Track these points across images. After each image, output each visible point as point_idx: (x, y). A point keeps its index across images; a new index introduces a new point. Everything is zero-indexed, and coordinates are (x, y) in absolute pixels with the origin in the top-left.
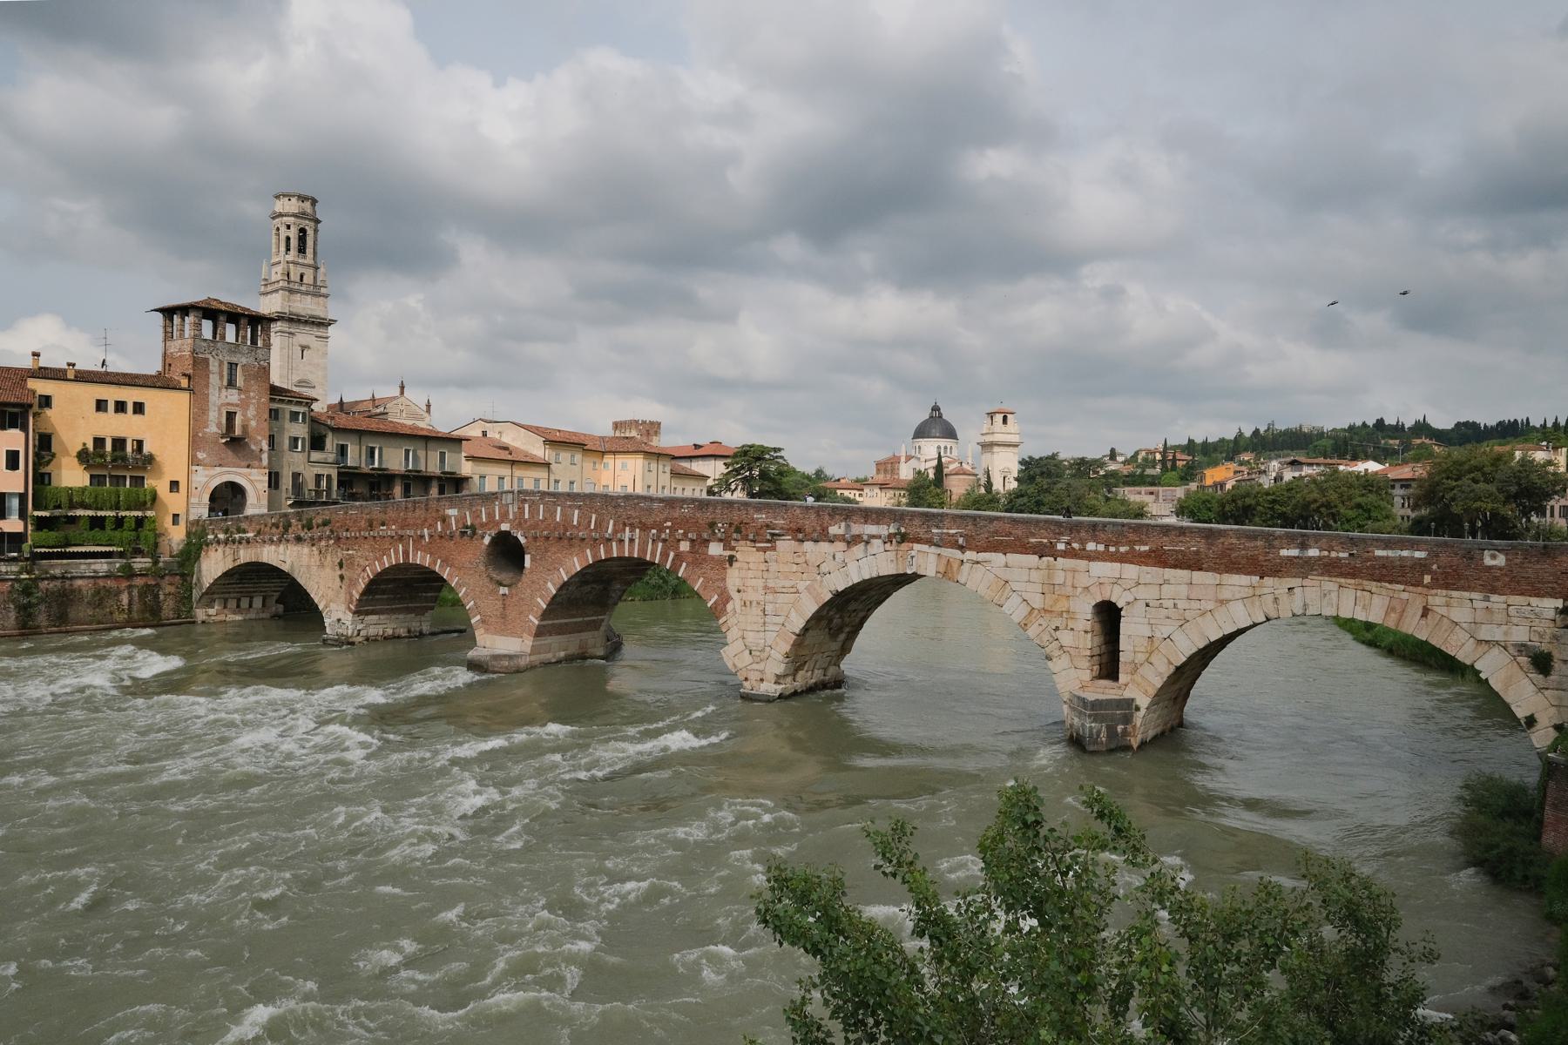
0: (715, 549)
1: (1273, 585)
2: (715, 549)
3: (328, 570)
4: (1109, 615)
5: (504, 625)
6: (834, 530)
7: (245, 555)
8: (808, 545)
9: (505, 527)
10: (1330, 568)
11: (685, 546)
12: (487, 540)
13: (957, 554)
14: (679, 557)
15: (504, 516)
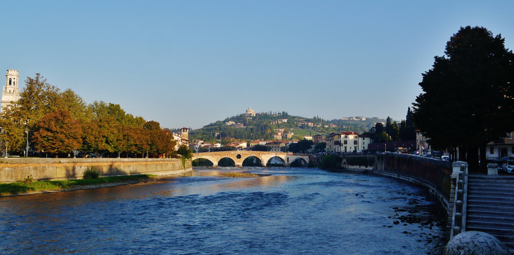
0: (261, 155)
1: (297, 156)
2: (261, 155)
3: (214, 159)
4: (288, 158)
5: (239, 162)
6: (271, 153)
7: (199, 157)
8: (268, 155)
9: (239, 154)
10: (299, 155)
11: (258, 155)
12: (237, 155)
13: (279, 155)
14: (258, 156)
15: (239, 153)
